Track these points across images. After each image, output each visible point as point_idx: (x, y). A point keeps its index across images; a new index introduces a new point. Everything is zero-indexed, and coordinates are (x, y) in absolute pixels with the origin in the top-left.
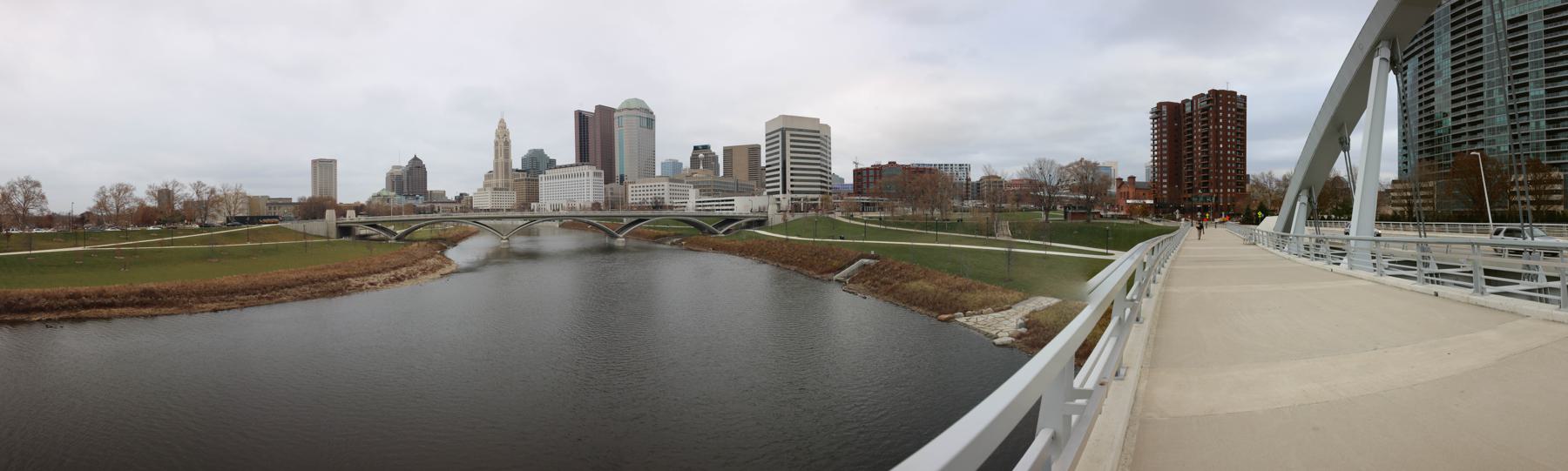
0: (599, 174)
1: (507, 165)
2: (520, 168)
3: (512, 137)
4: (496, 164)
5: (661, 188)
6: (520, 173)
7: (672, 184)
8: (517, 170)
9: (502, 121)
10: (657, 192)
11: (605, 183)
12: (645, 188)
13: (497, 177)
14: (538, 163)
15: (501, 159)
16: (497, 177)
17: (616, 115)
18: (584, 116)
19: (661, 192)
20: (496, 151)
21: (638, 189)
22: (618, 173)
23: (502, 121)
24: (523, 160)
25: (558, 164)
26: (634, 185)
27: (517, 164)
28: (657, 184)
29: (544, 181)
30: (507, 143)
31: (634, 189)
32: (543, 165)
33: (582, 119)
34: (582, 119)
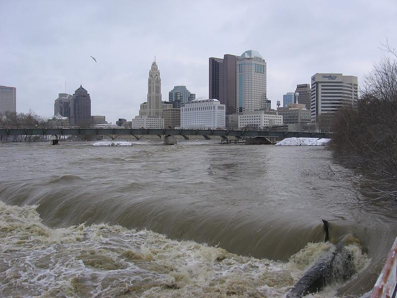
0: (222, 108)
1: (159, 97)
2: (168, 101)
3: (162, 77)
4: (149, 98)
5: (259, 118)
7: (266, 115)
8: (165, 102)
9: (154, 64)
10: (256, 121)
11: (227, 113)
12: (249, 118)
13: (150, 108)
14: (180, 98)
15: (154, 93)
16: (150, 108)
17: (238, 63)
18: (216, 62)
19: (259, 121)
20: (150, 88)
21: (244, 121)
22: (238, 107)
23: (154, 64)
24: (171, 94)
25: (197, 98)
26: (242, 116)
27: (165, 97)
28: (256, 115)
29: (184, 112)
30: (158, 81)
31: (242, 118)
32: (185, 100)
33: (214, 64)
34: (214, 64)
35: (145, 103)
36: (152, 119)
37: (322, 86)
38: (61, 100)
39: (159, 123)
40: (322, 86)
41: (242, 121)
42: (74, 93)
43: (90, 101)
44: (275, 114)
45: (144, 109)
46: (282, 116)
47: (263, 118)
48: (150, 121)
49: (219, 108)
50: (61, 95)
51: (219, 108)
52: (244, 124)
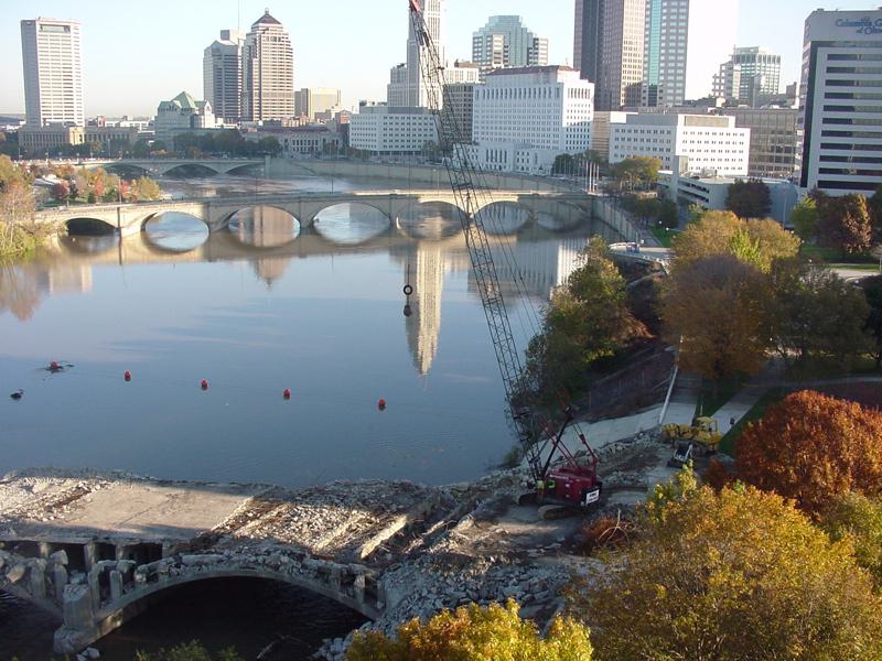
0: (584, 93)
5: (667, 137)
6: (465, 70)
35: (403, 65)
36: (400, 116)
37: (831, 57)
38: (218, 50)
39: (423, 133)
40: (831, 57)
41: (620, 143)
42: (249, 31)
43: (290, 51)
44: (727, 125)
45: (399, 81)
46: (747, 131)
47: (680, 137)
48: (393, 121)
49: (575, 93)
50: (225, 34)
51: (575, 93)
52: (626, 153)
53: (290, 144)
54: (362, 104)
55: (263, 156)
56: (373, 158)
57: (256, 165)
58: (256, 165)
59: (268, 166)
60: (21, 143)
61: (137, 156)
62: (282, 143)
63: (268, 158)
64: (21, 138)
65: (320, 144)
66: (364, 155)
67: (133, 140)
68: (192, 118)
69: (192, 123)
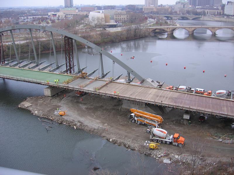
53: (209, 13)
54: (228, 2)
55: (202, 15)
56: (230, 17)
57: (200, 18)
58: (200, 18)
59: (202, 18)
60: (143, 10)
61: (170, 15)
62: (206, 12)
63: (203, 16)
64: (143, 9)
65: (216, 12)
66: (228, 16)
67: (170, 10)
68: (184, 5)
69: (184, 7)
